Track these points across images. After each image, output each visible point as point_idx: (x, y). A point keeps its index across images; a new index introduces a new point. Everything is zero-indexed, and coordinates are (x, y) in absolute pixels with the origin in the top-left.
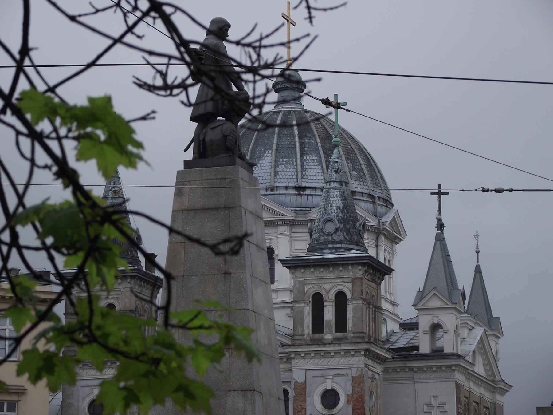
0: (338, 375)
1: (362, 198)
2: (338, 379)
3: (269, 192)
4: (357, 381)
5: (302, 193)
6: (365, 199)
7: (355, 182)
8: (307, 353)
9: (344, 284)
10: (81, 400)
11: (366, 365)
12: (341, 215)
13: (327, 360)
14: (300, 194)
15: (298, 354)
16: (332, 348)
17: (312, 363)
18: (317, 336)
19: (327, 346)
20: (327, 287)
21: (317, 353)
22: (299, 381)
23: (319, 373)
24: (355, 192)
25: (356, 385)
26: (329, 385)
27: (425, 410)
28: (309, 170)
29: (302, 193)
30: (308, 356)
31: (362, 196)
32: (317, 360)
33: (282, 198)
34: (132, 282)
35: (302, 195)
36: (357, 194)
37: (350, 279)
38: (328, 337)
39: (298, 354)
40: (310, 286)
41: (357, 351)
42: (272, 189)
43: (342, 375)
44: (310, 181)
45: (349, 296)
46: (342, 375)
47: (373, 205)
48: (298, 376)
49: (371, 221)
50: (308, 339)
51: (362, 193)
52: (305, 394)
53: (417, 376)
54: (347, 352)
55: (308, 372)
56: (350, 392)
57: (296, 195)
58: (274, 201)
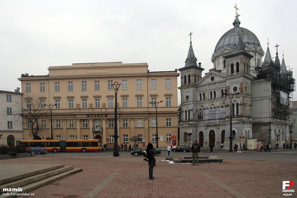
0: (237, 83)
2: (237, 84)
3: (228, 46)
4: (241, 84)
8: (229, 79)
11: (244, 80)
13: (234, 80)
15: (227, 79)
17: (231, 81)
21: (232, 78)
23: (232, 83)
24: (249, 43)
30: (230, 79)
39: (227, 79)
41: (241, 76)
42: (229, 45)
43: (238, 83)
46: (238, 83)
48: (228, 85)
54: (239, 77)
58: (229, 47)
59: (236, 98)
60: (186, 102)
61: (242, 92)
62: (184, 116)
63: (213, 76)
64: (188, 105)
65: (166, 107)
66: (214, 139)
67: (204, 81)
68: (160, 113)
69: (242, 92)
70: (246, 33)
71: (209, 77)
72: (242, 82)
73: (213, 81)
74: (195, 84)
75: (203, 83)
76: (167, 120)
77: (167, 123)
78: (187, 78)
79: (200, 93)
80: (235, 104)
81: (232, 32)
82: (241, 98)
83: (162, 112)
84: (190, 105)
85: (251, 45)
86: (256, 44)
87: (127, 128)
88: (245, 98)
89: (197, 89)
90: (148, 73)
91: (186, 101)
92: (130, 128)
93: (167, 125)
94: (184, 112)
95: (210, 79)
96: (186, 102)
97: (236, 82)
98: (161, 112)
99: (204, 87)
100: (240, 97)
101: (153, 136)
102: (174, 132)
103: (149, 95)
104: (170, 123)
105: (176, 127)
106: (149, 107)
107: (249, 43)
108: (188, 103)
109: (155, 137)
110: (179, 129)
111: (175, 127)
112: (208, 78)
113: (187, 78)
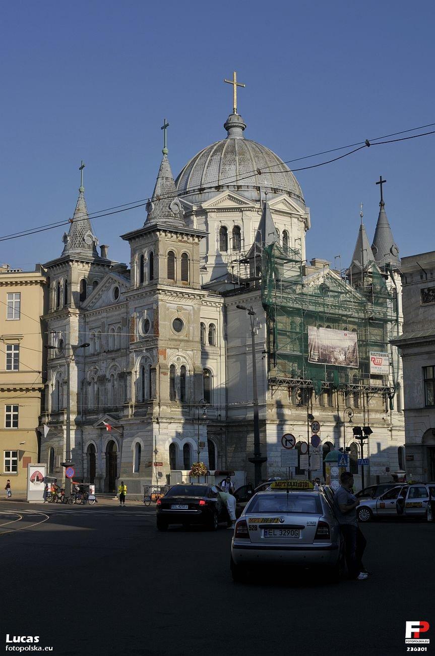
5: (202, 192)
14: (201, 193)
16: (142, 291)
24: (241, 186)
29: (202, 192)
31: (248, 188)
33: (190, 197)
63: (116, 285)
65: (6, 373)
71: (108, 288)
76: (8, 409)
77: (8, 417)
85: (246, 194)
93: (8, 424)
95: (111, 293)
99: (100, 317)
100: (152, 348)
104: (16, 417)
105: (31, 430)
107: (239, 187)
112: (108, 290)
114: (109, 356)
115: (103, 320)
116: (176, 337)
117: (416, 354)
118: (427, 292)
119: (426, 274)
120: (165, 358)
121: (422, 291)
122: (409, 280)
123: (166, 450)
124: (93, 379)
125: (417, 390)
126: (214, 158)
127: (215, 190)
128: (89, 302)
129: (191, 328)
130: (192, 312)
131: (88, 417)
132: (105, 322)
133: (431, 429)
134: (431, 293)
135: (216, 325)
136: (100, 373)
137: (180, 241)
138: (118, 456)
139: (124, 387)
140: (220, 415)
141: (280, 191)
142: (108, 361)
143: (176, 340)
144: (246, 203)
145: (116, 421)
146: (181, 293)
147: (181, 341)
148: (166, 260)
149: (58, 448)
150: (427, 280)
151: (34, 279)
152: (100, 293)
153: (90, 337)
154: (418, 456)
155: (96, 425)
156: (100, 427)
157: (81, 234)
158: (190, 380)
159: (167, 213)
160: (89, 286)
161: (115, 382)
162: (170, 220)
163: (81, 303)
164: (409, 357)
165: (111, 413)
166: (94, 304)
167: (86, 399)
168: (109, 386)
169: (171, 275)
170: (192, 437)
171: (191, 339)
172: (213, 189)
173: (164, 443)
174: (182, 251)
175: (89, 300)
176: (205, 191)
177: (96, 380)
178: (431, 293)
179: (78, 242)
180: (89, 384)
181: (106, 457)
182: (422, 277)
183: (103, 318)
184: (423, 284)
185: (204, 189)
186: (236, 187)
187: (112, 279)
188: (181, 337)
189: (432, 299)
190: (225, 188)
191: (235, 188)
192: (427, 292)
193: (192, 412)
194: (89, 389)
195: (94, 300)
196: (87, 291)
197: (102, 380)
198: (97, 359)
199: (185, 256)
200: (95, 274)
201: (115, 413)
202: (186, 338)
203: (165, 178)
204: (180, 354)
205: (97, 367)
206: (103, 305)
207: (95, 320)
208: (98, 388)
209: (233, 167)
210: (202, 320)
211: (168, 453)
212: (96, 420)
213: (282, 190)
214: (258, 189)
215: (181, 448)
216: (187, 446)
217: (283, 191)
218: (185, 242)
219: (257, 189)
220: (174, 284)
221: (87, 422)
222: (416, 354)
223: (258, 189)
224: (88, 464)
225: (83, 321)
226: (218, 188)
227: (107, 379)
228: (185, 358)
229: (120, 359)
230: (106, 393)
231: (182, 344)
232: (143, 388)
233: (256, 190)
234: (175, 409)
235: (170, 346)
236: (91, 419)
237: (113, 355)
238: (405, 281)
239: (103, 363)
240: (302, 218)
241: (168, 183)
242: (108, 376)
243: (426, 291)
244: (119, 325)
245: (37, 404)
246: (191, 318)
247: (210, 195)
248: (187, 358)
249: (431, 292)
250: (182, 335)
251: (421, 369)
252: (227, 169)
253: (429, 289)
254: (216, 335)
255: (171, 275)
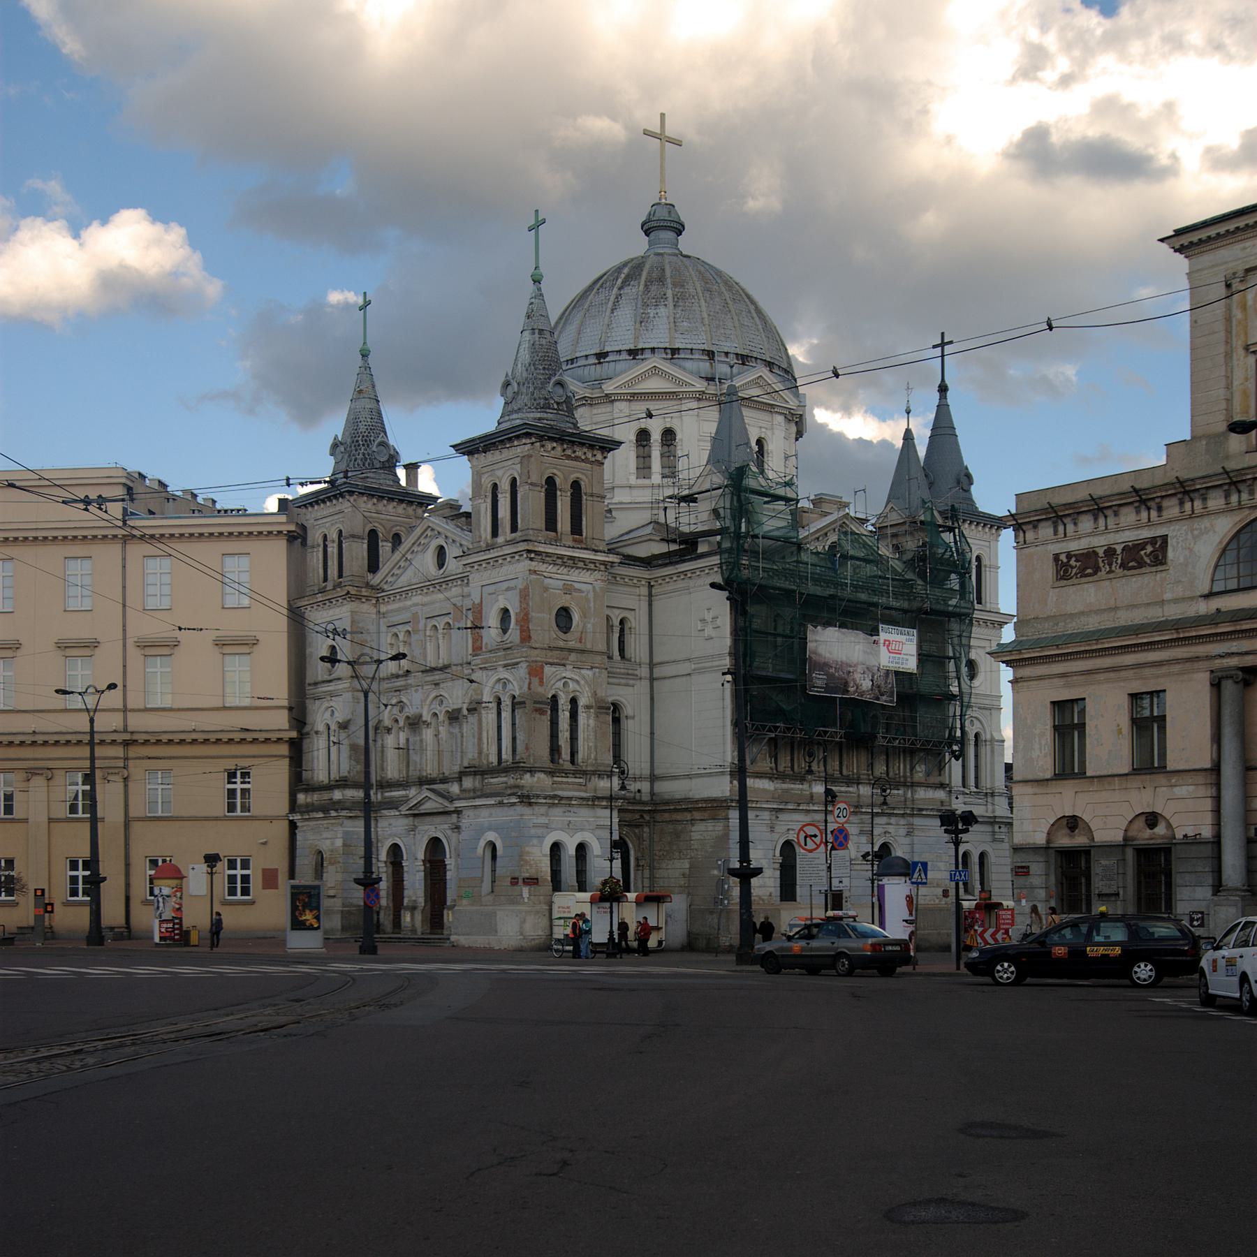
0: (508, 589)
1: (690, 357)
3: (570, 366)
6: (696, 356)
7: (681, 336)
9: (514, 466)
10: (319, 647)
12: (525, 375)
14: (600, 363)
16: (496, 555)
18: (495, 539)
19: (492, 551)
20: (499, 473)
22: (476, 602)
24: (679, 349)
25: (522, 600)
26: (502, 603)
27: (699, 628)
28: (616, 330)
29: (602, 360)
31: (692, 353)
32: (489, 572)
33: (580, 371)
34: (352, 499)
35: (602, 363)
36: (681, 351)
37: (519, 459)
38: (500, 540)
40: (486, 475)
44: (616, 343)
45: (518, 484)
47: (711, 364)
49: (698, 386)
50: (484, 545)
51: (692, 349)
52: (481, 617)
53: (691, 583)
55: (484, 588)
56: (518, 611)
57: (595, 364)
59: (505, 666)
60: (324, 682)
61: (526, 637)
62: (318, 758)
63: (441, 541)
64: (332, 695)
66: (444, 882)
67: (405, 569)
68: (189, 737)
69: (526, 637)
70: (669, 293)
71: (426, 546)
72: (526, 588)
73: (442, 571)
74: (368, 585)
75: (403, 580)
76: (231, 775)
77: (232, 793)
78: (333, 550)
79: (394, 630)
80: (507, 702)
81: (601, 286)
82: (522, 670)
83: (200, 737)
84: (340, 699)
85: (688, 364)
86: (727, 354)
87: (12, 821)
88: (548, 670)
89: (383, 609)
90: (124, 522)
91: (327, 677)
92: (26, 821)
93: (232, 807)
94: (317, 733)
95: (430, 557)
96: (324, 682)
97: (505, 585)
98: (194, 736)
99: (408, 603)
100: (517, 663)
101: (74, 865)
102: (265, 843)
103: (130, 642)
106: (129, 707)
107: (675, 351)
108: (331, 687)
109: (81, 873)
110: (293, 826)
111: (271, 819)
112: (424, 551)
113: (333, 550)
114: (428, 679)
115: (414, 609)
116: (561, 644)
117: (1040, 678)
118: (1065, 560)
119: (1065, 525)
120: (541, 683)
121: (1056, 557)
122: (1030, 535)
123: (545, 856)
124: (397, 721)
125: (1040, 744)
126: (626, 291)
127: (628, 357)
128: (387, 575)
129: (589, 626)
130: (591, 595)
131: (387, 794)
132: (420, 614)
133: (1064, 816)
134: (1073, 562)
135: (632, 620)
136: (410, 711)
137: (568, 457)
138: (448, 867)
139: (459, 735)
140: (639, 791)
141: (753, 360)
142: (425, 687)
143: (561, 649)
144: (688, 384)
145: (447, 804)
146: (571, 558)
147: (571, 650)
148: (543, 494)
149: (332, 851)
150: (1065, 536)
151: (275, 529)
152: (409, 556)
153: (389, 642)
154: (1037, 868)
155: (404, 809)
156: (411, 812)
157: (366, 441)
158: (588, 725)
159: (542, 402)
160: (385, 544)
161: (441, 728)
162: (550, 416)
163: (370, 576)
164: (1025, 684)
165: (432, 786)
166: (395, 577)
167: (383, 761)
168: (428, 734)
169: (551, 523)
170: (592, 831)
171: (589, 646)
172: (625, 356)
173: (541, 843)
174: (573, 477)
175: (387, 572)
176: (607, 359)
177: (401, 723)
178: (1073, 562)
179: (361, 456)
180: (389, 730)
181: (425, 868)
182: (1056, 533)
183: (415, 605)
184: (1058, 545)
185: (606, 354)
186: (669, 351)
187: (433, 530)
188: (572, 644)
189: (1076, 574)
190: (647, 354)
191: (667, 354)
192: (1065, 560)
193: (590, 785)
194: (389, 741)
195: (396, 571)
196: (381, 552)
197: (415, 723)
198: (403, 683)
199: (576, 485)
200: (395, 521)
201: (441, 786)
202: (579, 646)
203: (537, 331)
204: (568, 674)
205: (404, 700)
206: (414, 581)
207: (399, 610)
208: (408, 740)
209: (662, 311)
210: (608, 612)
211: (547, 861)
212: (406, 799)
213: (756, 358)
214: (711, 355)
215: (571, 851)
216: (581, 848)
217: (758, 361)
218: (577, 459)
219: (708, 355)
220: (556, 541)
221: (385, 803)
222: (1040, 678)
223: (711, 355)
224: (387, 881)
225: (375, 611)
226: (634, 353)
227: (426, 721)
228: (577, 682)
229: (450, 684)
230: (422, 750)
231: (573, 657)
232: (500, 739)
233: (706, 358)
234: (560, 779)
235: (551, 661)
236: (392, 797)
237: (437, 677)
238: (1021, 539)
239: (416, 691)
240: (793, 414)
241: (544, 342)
242: (427, 717)
243: (1063, 558)
244: (447, 619)
245: (283, 767)
246: (590, 608)
247: (619, 366)
248: (582, 682)
249: (1073, 559)
250: (572, 640)
251: (1049, 705)
252: (651, 315)
253: (1069, 556)
254: (633, 640)
255: (551, 523)
